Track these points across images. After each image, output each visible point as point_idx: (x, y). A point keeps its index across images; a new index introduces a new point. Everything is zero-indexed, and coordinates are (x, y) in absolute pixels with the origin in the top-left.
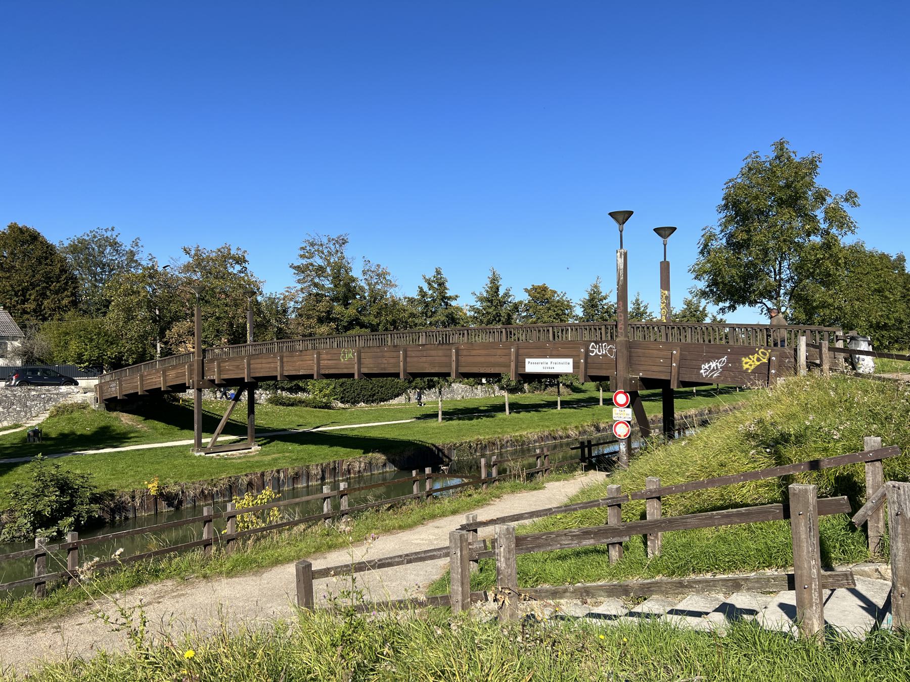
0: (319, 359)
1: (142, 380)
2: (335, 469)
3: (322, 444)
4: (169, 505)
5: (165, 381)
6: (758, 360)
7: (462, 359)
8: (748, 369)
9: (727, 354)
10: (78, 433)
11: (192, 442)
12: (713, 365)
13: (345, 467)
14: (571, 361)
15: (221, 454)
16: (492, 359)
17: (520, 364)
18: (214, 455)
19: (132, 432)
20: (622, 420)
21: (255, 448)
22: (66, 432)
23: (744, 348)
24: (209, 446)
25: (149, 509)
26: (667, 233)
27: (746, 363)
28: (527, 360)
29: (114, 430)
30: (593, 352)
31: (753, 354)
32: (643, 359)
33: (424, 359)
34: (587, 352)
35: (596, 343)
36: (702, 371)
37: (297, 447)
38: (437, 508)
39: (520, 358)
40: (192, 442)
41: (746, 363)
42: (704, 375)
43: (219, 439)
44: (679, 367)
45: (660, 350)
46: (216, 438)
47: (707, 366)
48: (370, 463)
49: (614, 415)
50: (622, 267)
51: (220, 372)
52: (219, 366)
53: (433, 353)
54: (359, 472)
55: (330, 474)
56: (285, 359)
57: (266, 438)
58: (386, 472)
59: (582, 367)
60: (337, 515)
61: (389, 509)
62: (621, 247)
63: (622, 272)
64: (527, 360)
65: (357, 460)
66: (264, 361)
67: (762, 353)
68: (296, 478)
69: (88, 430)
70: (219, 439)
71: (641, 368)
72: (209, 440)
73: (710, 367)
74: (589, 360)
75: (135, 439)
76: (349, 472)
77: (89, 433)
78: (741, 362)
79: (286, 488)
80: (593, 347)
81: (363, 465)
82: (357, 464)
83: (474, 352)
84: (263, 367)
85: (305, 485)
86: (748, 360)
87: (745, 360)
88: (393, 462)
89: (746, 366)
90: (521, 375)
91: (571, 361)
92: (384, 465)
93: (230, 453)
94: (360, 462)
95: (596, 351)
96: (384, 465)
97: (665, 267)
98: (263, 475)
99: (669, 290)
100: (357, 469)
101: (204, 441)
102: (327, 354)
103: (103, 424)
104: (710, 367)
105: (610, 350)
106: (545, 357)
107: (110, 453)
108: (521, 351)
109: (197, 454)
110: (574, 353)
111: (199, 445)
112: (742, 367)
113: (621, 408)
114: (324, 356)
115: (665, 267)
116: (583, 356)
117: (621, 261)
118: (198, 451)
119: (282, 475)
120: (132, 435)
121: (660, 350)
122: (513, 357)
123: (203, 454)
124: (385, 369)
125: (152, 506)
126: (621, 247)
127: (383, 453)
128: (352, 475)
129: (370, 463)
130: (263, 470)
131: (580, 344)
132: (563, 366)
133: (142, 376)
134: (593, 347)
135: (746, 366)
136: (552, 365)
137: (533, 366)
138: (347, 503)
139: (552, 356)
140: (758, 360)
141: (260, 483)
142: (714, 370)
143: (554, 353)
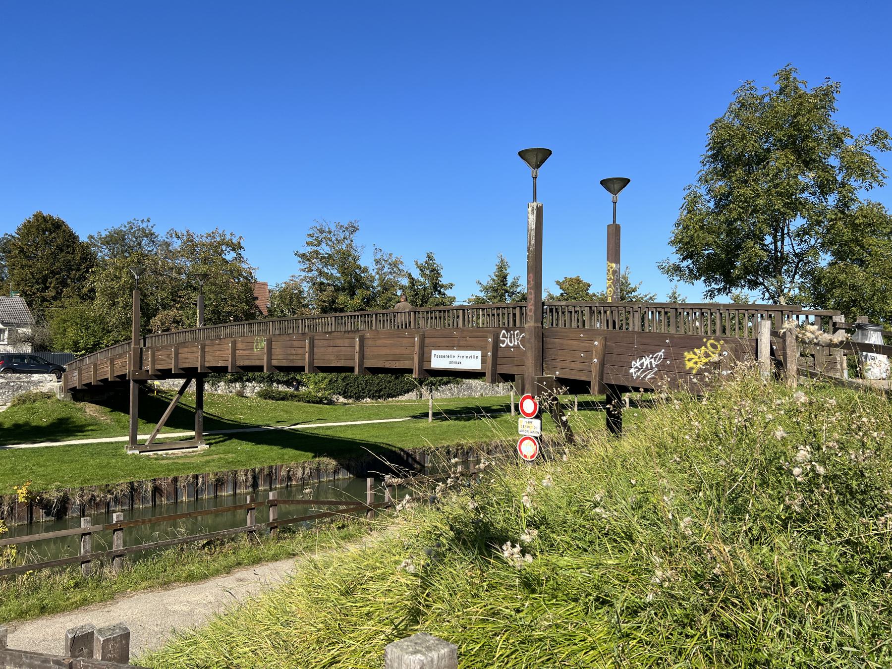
0: (234, 349)
1: (96, 370)
2: (270, 475)
3: (275, 445)
4: (48, 514)
5: (112, 370)
6: (707, 355)
7: (367, 350)
8: (691, 369)
9: (666, 346)
10: (34, 424)
11: (127, 438)
12: (646, 361)
13: (283, 473)
14: (479, 353)
15: (160, 453)
16: (397, 351)
17: (424, 357)
18: (151, 453)
19: (89, 425)
20: (529, 434)
21: (203, 447)
22: (21, 422)
23: (691, 338)
24: (147, 444)
25: (20, 518)
26: (617, 186)
27: (690, 360)
28: (434, 352)
29: (74, 422)
30: (503, 342)
31: (699, 347)
32: (560, 352)
33: (330, 350)
34: (496, 342)
35: (508, 330)
36: (632, 371)
37: (248, 446)
38: (288, 545)
39: (426, 349)
40: (127, 438)
41: (690, 360)
42: (635, 376)
43: (159, 436)
44: (602, 364)
45: (580, 340)
46: (155, 435)
47: (638, 364)
48: (318, 469)
49: (520, 428)
50: (534, 227)
51: (154, 362)
52: (153, 356)
53: (339, 342)
54: (303, 478)
55: (265, 481)
56: (207, 349)
57: (225, 435)
58: (338, 479)
59: (489, 361)
60: (109, 556)
61: (204, 546)
62: (535, 199)
63: (533, 233)
64: (434, 352)
65: (297, 463)
66: (190, 350)
67: (712, 345)
68: (219, 483)
69: (44, 422)
70: (159, 436)
71: (559, 364)
72: (148, 437)
73: (642, 365)
74: (500, 354)
75: (89, 433)
76: (289, 478)
77: (44, 424)
78: (682, 359)
79: (205, 496)
80: (504, 336)
81: (307, 471)
82: (300, 471)
83: (379, 342)
84: (220, 356)
85: (231, 492)
86: (692, 355)
87: (688, 355)
88: (348, 468)
89: (689, 365)
90: (427, 371)
91: (479, 353)
92: (336, 472)
93: (170, 452)
94: (304, 468)
95: (507, 341)
96: (336, 472)
97: (614, 233)
98: (175, 480)
99: (617, 261)
100: (299, 475)
101: (139, 437)
102: (242, 342)
103: (63, 415)
104: (642, 365)
105: (523, 341)
106: (451, 348)
107: (47, 447)
108: (427, 341)
109: (130, 453)
110: (483, 344)
111: (134, 441)
112: (684, 365)
113: (528, 419)
114: (239, 345)
115: (614, 233)
116: (490, 347)
117: (532, 218)
118: (131, 449)
119: (200, 481)
120: (90, 428)
121: (580, 340)
122: (417, 349)
123: (137, 452)
124: (293, 361)
125: (25, 515)
126: (535, 199)
127: (334, 458)
128: (294, 483)
129: (318, 469)
130: (175, 474)
131: (488, 332)
132: (471, 360)
133: (96, 365)
134: (504, 336)
135: (689, 365)
136: (456, 359)
137: (441, 360)
138: (121, 542)
139: (461, 348)
140: (707, 355)
141: (171, 489)
142: (647, 369)
143: (462, 343)
